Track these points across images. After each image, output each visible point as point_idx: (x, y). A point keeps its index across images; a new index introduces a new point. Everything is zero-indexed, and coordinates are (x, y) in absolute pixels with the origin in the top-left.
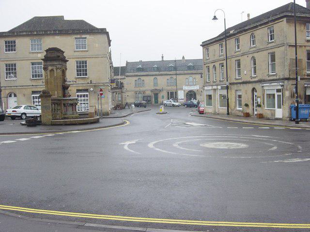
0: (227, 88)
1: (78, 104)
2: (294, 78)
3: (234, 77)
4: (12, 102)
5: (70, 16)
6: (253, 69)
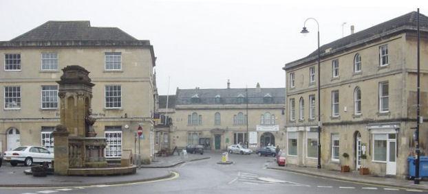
0: (319, 130)
1: (107, 147)
2: (412, 119)
3: (329, 114)
4: (13, 141)
5: (99, 20)
6: (356, 105)
